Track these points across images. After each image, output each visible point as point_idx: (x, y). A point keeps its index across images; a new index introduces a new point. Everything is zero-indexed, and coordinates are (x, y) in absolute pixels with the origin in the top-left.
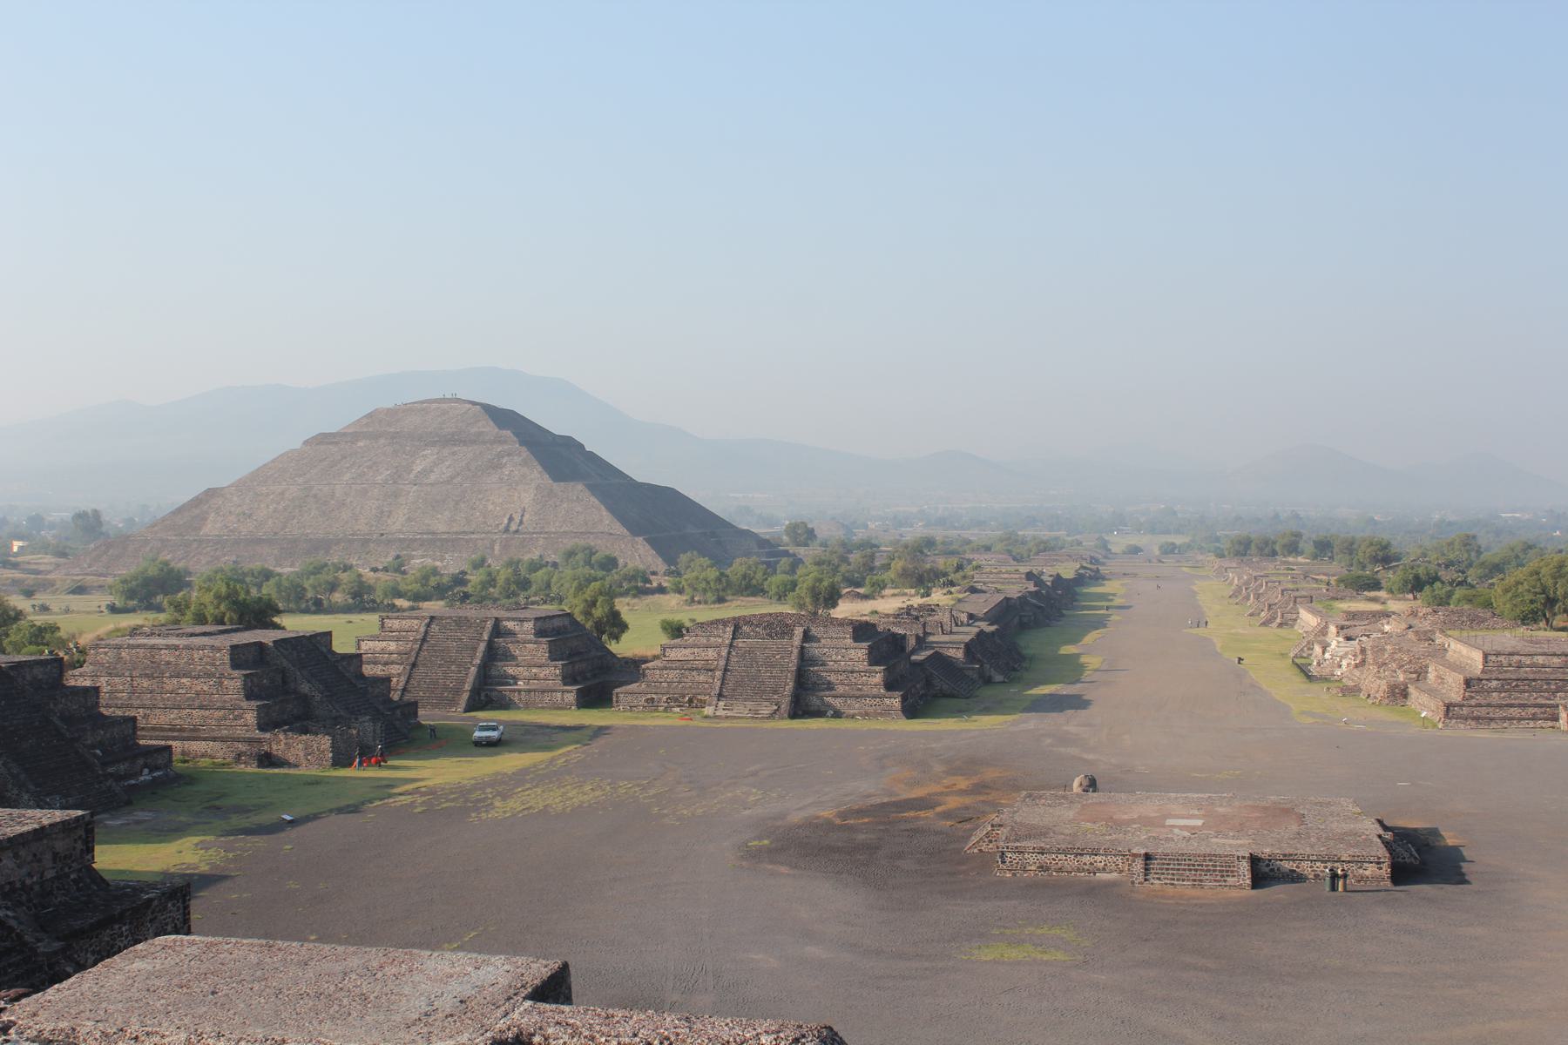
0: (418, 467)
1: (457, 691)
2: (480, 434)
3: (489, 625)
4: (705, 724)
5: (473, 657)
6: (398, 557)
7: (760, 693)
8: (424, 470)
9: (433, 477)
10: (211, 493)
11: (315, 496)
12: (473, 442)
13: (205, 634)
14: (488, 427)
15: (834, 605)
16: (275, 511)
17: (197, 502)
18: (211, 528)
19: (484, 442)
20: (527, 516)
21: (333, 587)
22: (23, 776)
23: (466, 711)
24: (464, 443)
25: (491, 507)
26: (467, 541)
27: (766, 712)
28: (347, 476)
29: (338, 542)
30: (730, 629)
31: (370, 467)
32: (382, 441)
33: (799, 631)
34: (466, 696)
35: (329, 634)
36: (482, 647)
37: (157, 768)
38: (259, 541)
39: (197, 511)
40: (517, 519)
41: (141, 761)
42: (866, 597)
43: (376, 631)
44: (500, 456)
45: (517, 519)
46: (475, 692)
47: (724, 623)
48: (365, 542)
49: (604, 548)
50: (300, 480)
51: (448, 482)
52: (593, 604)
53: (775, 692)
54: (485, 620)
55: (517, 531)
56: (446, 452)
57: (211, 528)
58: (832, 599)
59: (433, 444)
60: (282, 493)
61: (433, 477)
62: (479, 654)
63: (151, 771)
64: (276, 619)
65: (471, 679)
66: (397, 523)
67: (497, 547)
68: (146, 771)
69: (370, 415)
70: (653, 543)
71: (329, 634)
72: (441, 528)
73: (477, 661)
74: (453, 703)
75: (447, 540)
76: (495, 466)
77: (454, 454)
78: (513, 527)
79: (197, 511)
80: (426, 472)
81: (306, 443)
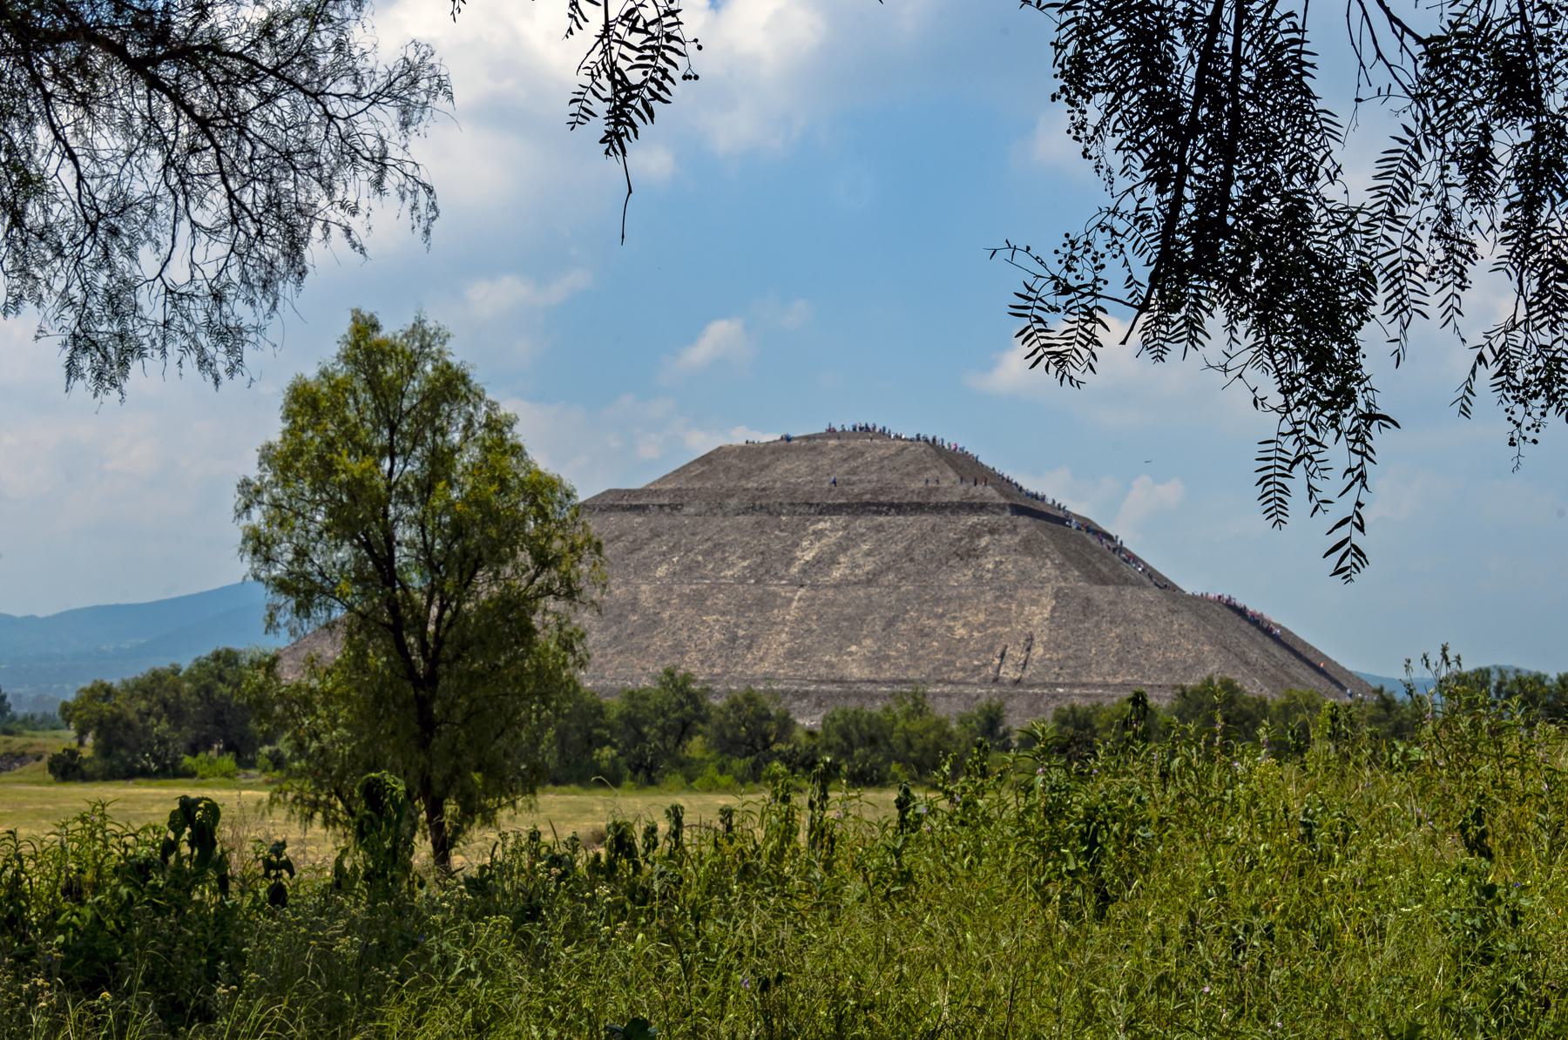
2: (930, 491)
8: (818, 560)
12: (918, 508)
19: (939, 508)
20: (1038, 651)
24: (899, 508)
25: (961, 632)
28: (661, 571)
31: (706, 553)
32: (733, 502)
44: (974, 533)
51: (871, 579)
55: (1017, 682)
56: (861, 524)
59: (836, 509)
61: (836, 574)
72: (855, 671)
77: (879, 529)
78: (1009, 673)
80: (824, 562)
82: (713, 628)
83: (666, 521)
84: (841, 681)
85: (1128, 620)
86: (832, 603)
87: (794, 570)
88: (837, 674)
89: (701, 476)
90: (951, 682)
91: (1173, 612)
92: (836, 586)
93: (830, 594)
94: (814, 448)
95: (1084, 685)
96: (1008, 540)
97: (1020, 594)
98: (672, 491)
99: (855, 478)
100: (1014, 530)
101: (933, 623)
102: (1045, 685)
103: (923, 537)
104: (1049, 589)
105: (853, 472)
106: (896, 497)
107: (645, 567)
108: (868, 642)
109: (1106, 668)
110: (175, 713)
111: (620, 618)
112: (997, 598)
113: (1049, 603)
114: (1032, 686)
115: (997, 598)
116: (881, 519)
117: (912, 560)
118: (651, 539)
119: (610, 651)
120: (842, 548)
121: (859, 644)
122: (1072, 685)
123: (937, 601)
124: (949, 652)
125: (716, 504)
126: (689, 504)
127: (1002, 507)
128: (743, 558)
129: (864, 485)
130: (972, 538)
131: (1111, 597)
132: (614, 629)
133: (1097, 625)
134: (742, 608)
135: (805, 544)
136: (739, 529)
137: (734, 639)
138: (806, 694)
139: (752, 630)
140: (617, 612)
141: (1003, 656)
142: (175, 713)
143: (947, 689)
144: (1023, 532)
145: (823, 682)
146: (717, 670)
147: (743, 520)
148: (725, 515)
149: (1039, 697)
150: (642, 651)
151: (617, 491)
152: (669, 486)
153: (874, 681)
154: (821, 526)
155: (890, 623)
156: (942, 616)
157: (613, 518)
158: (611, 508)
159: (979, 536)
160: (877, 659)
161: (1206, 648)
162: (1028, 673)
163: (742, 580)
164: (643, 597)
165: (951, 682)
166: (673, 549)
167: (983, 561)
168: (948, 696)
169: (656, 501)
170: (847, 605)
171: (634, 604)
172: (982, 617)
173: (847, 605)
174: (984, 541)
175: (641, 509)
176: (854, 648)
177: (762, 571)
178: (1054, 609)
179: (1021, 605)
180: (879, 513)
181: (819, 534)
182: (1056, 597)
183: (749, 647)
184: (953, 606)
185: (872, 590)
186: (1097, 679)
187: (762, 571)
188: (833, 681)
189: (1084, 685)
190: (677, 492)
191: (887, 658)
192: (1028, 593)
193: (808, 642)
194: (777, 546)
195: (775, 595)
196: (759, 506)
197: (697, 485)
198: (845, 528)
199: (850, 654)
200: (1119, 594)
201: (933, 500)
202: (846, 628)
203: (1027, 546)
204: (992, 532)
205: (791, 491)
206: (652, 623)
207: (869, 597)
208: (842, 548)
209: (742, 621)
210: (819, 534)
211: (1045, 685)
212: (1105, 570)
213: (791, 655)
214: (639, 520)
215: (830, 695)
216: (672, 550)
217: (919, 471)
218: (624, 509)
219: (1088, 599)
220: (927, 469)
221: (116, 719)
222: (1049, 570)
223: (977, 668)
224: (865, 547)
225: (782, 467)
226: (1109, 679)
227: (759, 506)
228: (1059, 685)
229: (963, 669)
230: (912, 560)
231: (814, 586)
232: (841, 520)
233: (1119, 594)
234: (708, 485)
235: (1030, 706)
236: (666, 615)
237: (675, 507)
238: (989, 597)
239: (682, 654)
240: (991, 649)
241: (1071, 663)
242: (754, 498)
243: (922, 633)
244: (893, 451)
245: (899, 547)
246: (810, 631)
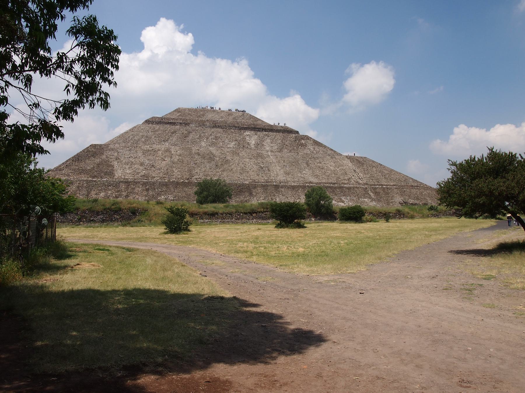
60: (168, 150)
81: (147, 122)
84: (310, 182)
125: (202, 124)
132: (213, 162)
157: (168, 126)
175: (174, 124)
176: (304, 172)
237: (187, 124)
245: (280, 141)
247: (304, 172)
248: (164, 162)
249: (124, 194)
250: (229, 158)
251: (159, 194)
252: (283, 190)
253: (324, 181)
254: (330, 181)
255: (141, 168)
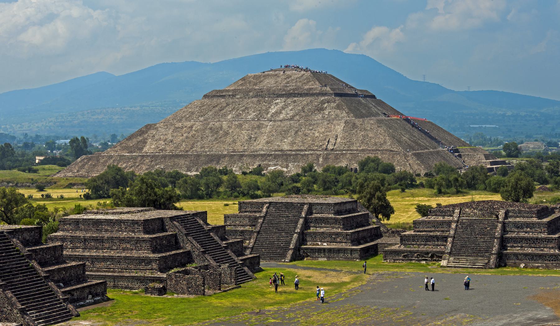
0: (273, 110)
1: (287, 249)
2: (311, 89)
3: (306, 207)
4: (440, 271)
5: (295, 228)
6: (260, 165)
7: (478, 252)
8: (276, 112)
9: (282, 116)
10: (149, 127)
11: (211, 129)
12: (306, 95)
13: (128, 213)
14: (316, 86)
15: (531, 196)
16: (187, 137)
17: (141, 132)
18: (149, 148)
19: (313, 95)
20: (339, 140)
21: (218, 185)
22: (14, 299)
23: (291, 261)
24: (301, 95)
25: (317, 134)
26: (303, 155)
27: (480, 264)
28: (229, 117)
29: (225, 156)
30: (457, 211)
31: (243, 111)
32: (251, 94)
33: (502, 213)
34: (290, 252)
35: (205, 213)
36: (301, 221)
37: (97, 295)
38: (177, 156)
39: (140, 138)
40: (332, 141)
41: (87, 291)
42: (551, 190)
43: (237, 212)
44: (323, 103)
45: (332, 141)
46: (297, 249)
47: (454, 206)
48: (242, 156)
49: (385, 158)
50: (202, 119)
51: (292, 119)
52: (372, 196)
53: (487, 251)
54: (304, 204)
55: (332, 150)
56: (289, 101)
57: (149, 148)
58: (528, 192)
60: (191, 127)
61: (282, 116)
62: (299, 226)
63: (93, 297)
64: (177, 205)
65: (294, 241)
66: (260, 145)
67: (321, 160)
68: (90, 296)
69: (243, 79)
70: (418, 156)
71: (205, 213)
72: (286, 147)
73: (298, 230)
74: (284, 256)
75: (290, 155)
76: (320, 109)
77: (295, 102)
78: (330, 147)
79: (140, 138)
81: (205, 96)
82: (244, 135)
83: (231, 101)
84: (282, 150)
85: (365, 130)
86: (280, 126)
87: (269, 116)
88: (280, 148)
89: (242, 85)
90: (313, 150)
91: (379, 127)
92: (281, 121)
93: (279, 123)
94: (276, 75)
95: (351, 150)
96: (333, 105)
97: (334, 123)
98: (233, 90)
99: (288, 85)
100: (334, 102)
101: (309, 132)
102: (340, 150)
103: (308, 104)
104: (343, 121)
105: (288, 83)
106: (300, 91)
107: (225, 115)
108: (290, 138)
109: (358, 145)
110: (108, 182)
111: (217, 133)
112: (328, 124)
113: (343, 125)
114: (336, 151)
115: (328, 124)
116: (295, 99)
117: (304, 112)
118: (226, 106)
119: (214, 143)
120: (283, 108)
121: (287, 139)
122: (348, 150)
123: (310, 125)
124: (313, 141)
125: (246, 94)
126: (238, 95)
127: (332, 94)
128: (254, 112)
129: (292, 86)
130: (322, 104)
131: (361, 123)
133: (356, 131)
134: (253, 128)
135: (272, 107)
136: (252, 102)
137: (251, 138)
138: (271, 155)
139: (256, 136)
140: (216, 130)
141: (328, 142)
142: (108, 182)
143: (312, 152)
144: (337, 102)
145: (276, 151)
146: (246, 148)
147: (255, 100)
148: (249, 98)
149: (338, 154)
150: (224, 142)
151: (216, 90)
152: (232, 88)
153: (291, 150)
154: (277, 101)
155: (296, 132)
156: (312, 129)
158: (214, 96)
159: (324, 104)
160: (292, 143)
161: (387, 138)
162: (335, 147)
163: (253, 120)
164: (224, 125)
165: (313, 150)
166: (234, 109)
167: (325, 111)
168: (312, 154)
169: (227, 94)
170: (284, 127)
171: (221, 128)
172: (323, 130)
173: (284, 127)
174: (325, 106)
175: (223, 96)
176: (286, 140)
177: (259, 117)
178: (344, 127)
179: (335, 126)
180: (295, 97)
181: (277, 104)
182: (345, 123)
183: (255, 141)
184: (315, 126)
185: (291, 122)
186: (355, 148)
187: (259, 116)
188: (279, 151)
189: (351, 150)
190: (234, 90)
191: (295, 143)
192: (337, 122)
193: (272, 139)
194: (264, 108)
195: (263, 124)
196: (260, 94)
197: (241, 88)
198: (284, 102)
199: (285, 142)
200: (363, 122)
201: (311, 92)
202: (284, 134)
203: (338, 107)
204: (328, 102)
205: (268, 90)
206: (227, 134)
207: (290, 124)
208: (283, 108)
209: (253, 132)
210: (277, 104)
211: (340, 150)
212: (364, 112)
213: (268, 143)
214: (223, 100)
215: (278, 155)
216: (233, 110)
217: (308, 82)
218: (218, 96)
219: (354, 123)
220: (310, 81)
221: (97, 186)
222: (344, 114)
223: (321, 145)
224: (290, 108)
225: (267, 81)
226: (359, 148)
227: (260, 94)
228: (344, 150)
229: (317, 146)
230: (304, 112)
231: (275, 121)
232: (283, 99)
233: (363, 122)
234: (244, 88)
235: (335, 157)
236: (230, 131)
238: (326, 123)
239: (235, 143)
240: (325, 139)
241: (348, 143)
242: (257, 92)
243: (305, 135)
244: (300, 75)
245: (300, 108)
246: (273, 135)
247: (286, 140)
248: (181, 138)
249: (137, 164)
250: (230, 131)
251: (156, 165)
252: (245, 158)
253: (294, 148)
254: (302, 148)
255: (163, 143)
